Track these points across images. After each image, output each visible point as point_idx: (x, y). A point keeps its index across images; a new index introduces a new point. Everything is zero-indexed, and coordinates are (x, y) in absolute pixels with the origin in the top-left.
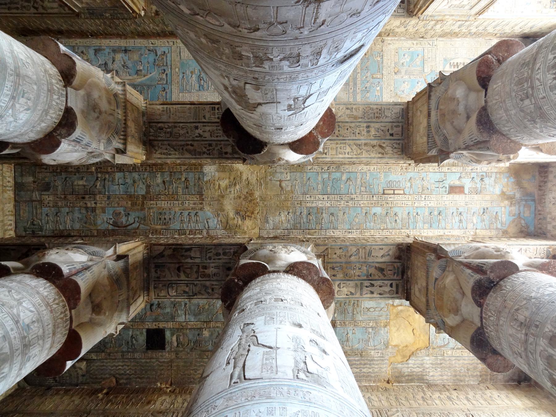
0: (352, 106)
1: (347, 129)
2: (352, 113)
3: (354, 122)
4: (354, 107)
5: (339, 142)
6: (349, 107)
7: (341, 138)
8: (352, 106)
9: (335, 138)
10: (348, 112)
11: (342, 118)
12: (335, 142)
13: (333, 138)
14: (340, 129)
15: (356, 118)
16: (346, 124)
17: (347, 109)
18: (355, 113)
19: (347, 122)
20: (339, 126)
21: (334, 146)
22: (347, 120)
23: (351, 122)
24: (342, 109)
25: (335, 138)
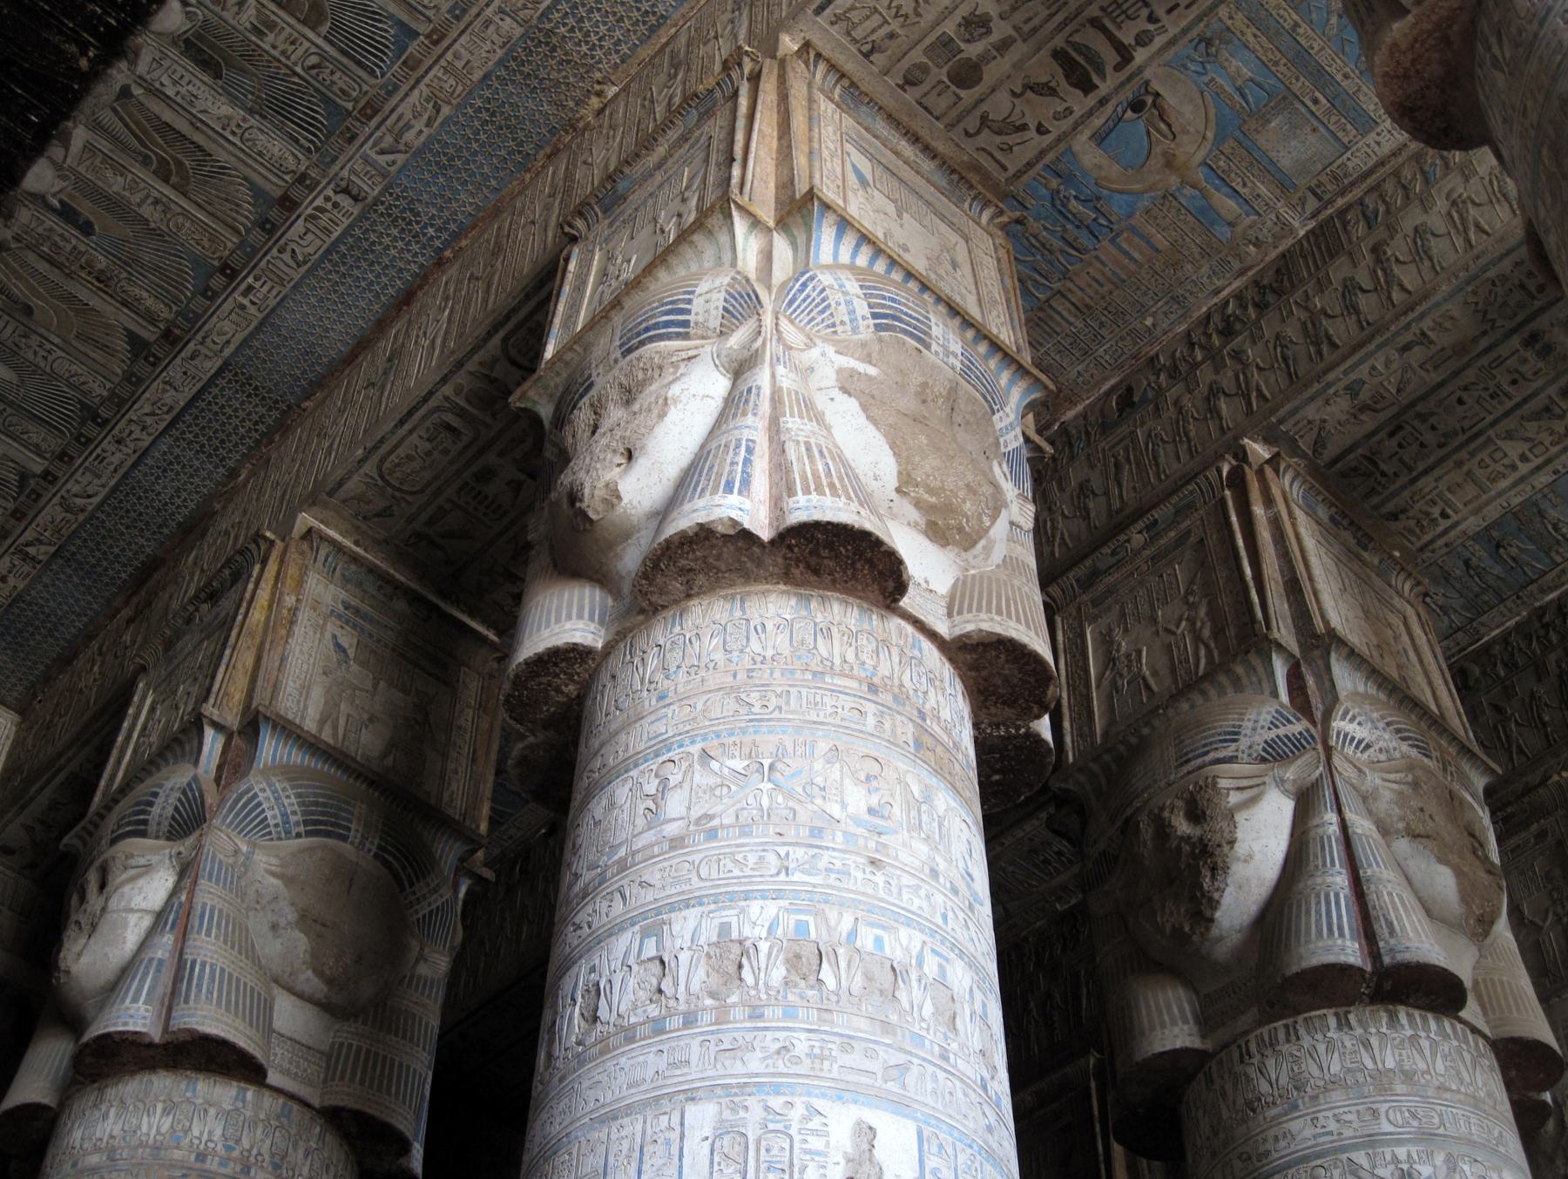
0: (1415, 329)
1: (1460, 402)
2: (1434, 349)
3: (1467, 365)
4: (1426, 324)
5: (1463, 454)
6: (1408, 337)
7: (1462, 438)
8: (1415, 329)
9: (1442, 452)
10: (1417, 355)
11: (1410, 388)
12: (1450, 463)
13: (1432, 459)
14: (1433, 420)
15: (1460, 349)
16: (1444, 393)
17: (1406, 348)
18: (1443, 340)
19: (1442, 384)
20: (1422, 417)
21: (1456, 476)
22: (1434, 378)
23: (1457, 373)
24: (1387, 364)
25: (1442, 452)
